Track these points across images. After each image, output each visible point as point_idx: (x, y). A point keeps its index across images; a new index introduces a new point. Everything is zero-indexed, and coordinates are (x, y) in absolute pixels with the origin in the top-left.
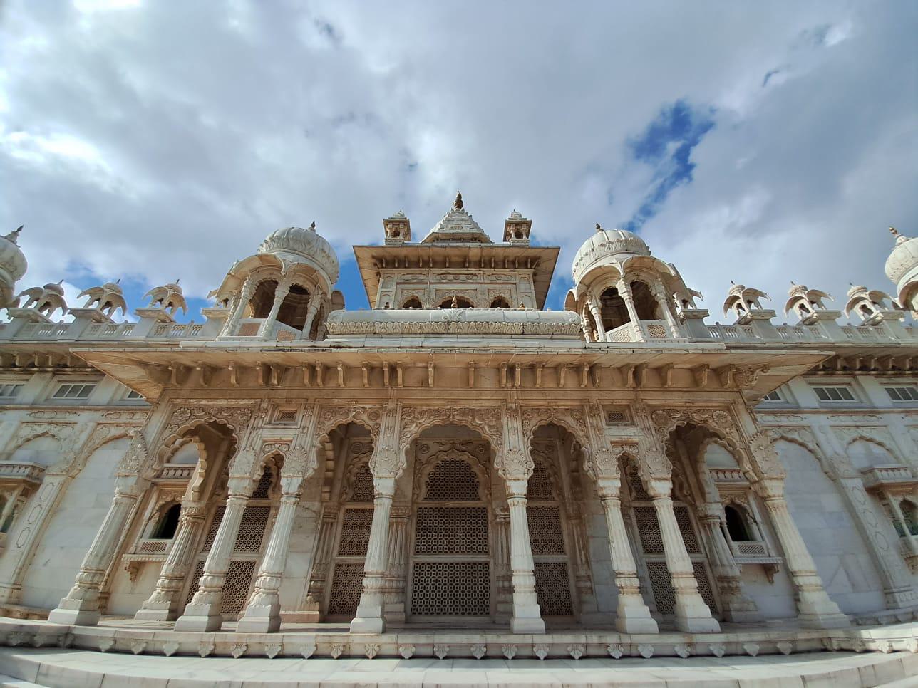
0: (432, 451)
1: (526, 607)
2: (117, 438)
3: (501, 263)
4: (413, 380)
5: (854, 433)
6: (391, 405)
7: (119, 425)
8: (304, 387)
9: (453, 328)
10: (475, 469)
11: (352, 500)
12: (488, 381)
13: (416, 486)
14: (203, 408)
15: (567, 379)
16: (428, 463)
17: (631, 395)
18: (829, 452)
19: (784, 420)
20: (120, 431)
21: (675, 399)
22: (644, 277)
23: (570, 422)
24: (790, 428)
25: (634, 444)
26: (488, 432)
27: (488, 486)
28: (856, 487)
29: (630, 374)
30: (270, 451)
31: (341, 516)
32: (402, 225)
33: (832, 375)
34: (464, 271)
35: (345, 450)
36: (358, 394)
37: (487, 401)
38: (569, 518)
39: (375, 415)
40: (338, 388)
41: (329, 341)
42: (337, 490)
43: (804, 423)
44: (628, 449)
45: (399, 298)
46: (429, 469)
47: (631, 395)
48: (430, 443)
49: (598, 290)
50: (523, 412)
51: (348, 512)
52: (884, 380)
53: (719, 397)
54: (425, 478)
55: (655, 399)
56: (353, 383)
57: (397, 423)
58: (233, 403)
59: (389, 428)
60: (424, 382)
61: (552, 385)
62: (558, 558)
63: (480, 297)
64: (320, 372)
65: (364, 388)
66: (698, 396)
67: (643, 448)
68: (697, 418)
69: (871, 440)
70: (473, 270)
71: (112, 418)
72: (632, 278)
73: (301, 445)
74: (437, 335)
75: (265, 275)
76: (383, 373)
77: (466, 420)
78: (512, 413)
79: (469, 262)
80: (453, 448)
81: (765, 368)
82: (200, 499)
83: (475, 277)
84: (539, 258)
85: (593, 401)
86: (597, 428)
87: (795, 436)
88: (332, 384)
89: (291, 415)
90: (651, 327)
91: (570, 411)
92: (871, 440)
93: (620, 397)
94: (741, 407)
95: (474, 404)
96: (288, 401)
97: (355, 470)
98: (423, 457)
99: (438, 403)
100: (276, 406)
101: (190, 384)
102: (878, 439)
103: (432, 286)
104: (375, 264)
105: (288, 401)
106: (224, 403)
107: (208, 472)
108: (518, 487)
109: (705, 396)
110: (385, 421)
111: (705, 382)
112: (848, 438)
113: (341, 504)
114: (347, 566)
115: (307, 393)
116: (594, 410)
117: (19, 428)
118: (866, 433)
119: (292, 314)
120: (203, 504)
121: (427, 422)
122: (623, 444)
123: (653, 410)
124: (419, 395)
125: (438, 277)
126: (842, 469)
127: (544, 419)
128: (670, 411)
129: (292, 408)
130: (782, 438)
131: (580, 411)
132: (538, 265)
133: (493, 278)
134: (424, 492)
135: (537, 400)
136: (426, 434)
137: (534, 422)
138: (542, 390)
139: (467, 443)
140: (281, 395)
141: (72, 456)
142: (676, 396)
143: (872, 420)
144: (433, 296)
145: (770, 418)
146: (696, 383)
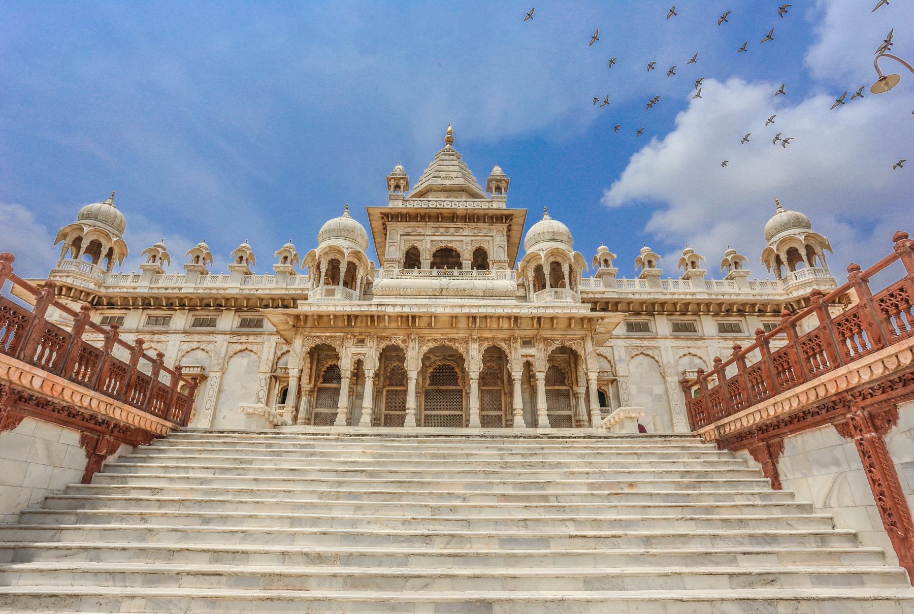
0: (433, 360)
2: (241, 351)
3: (482, 218)
4: (423, 324)
5: (686, 351)
6: (413, 337)
7: (241, 343)
8: (367, 327)
9: (444, 293)
10: (457, 370)
11: (389, 385)
12: (463, 324)
13: (424, 378)
14: (318, 337)
15: (505, 324)
16: (430, 366)
17: (536, 332)
18: (665, 361)
20: (243, 347)
21: (557, 334)
22: (559, 259)
23: (503, 345)
25: (533, 356)
26: (461, 350)
27: (464, 379)
28: (673, 382)
29: (535, 321)
30: (356, 358)
31: (385, 393)
32: (402, 181)
33: (684, 314)
34: (452, 225)
35: (383, 359)
36: (396, 331)
37: (462, 334)
38: (505, 394)
39: (404, 341)
40: (385, 328)
41: (376, 300)
42: (382, 379)
43: (657, 345)
44: (530, 359)
45: (402, 248)
46: (431, 370)
47: (536, 332)
48: (431, 356)
49: (533, 265)
50: (481, 340)
51: (388, 391)
52: (719, 318)
53: (579, 333)
54: (428, 375)
55: (547, 334)
56: (393, 325)
57: (417, 346)
58: (333, 334)
59: (413, 348)
60: (430, 325)
61: (496, 326)
62: (499, 413)
63: (465, 248)
64: (374, 319)
65: (398, 328)
66: (570, 332)
67: (537, 357)
68: (567, 344)
69: (695, 355)
70: (459, 225)
71: (236, 339)
72: (552, 259)
73: (371, 354)
74: (435, 296)
75: (332, 256)
76: (409, 320)
77: (451, 344)
78: (474, 341)
79: (457, 217)
80: (444, 358)
81: (602, 319)
82: (310, 383)
83: (461, 230)
84: (512, 215)
85: (516, 335)
86: (516, 349)
87: (650, 352)
88: (382, 325)
89: (362, 341)
90: (556, 292)
91: (504, 340)
92: (695, 355)
93: (530, 333)
94: (589, 339)
95: (455, 336)
96: (361, 334)
97: (389, 370)
98: (427, 363)
99: (438, 335)
100: (354, 336)
101: (309, 324)
102: (699, 355)
103: (428, 238)
104: (383, 218)
105: (361, 334)
106: (328, 334)
107: (311, 369)
109: (573, 332)
111: (573, 326)
112: (681, 354)
113: (384, 387)
114: (391, 415)
115: (369, 330)
116: (515, 339)
117: (180, 345)
118: (693, 351)
119: (350, 282)
120: (312, 385)
121: (432, 345)
122: (526, 356)
123: (546, 339)
124: (426, 331)
125: (433, 230)
126: (669, 371)
127: (490, 344)
128: (553, 340)
129: (363, 337)
130: (642, 353)
132: (511, 220)
133: (476, 231)
134: (428, 381)
135: (487, 334)
136: (431, 351)
137: (486, 345)
138: (490, 329)
139: (452, 356)
140: (357, 330)
141: (221, 361)
142: (558, 332)
143: (699, 343)
144: (429, 247)
145: (638, 341)
146: (570, 325)
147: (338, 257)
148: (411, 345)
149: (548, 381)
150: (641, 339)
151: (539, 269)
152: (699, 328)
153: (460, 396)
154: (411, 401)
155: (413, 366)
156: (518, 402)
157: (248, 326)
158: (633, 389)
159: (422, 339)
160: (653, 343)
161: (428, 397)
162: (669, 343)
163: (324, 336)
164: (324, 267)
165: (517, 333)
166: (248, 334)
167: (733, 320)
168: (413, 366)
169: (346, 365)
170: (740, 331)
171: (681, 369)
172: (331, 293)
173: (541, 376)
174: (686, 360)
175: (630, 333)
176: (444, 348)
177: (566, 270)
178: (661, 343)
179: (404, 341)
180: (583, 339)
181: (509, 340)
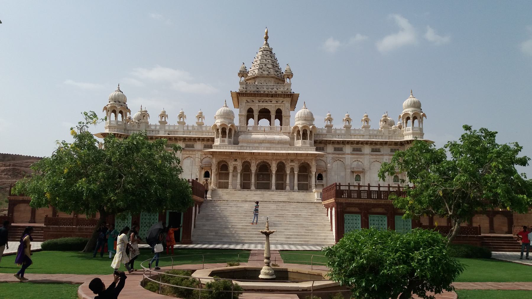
1: (274, 187)
19: (340, 156)
21: (303, 158)
22: (306, 128)
23: (284, 161)
24: (341, 158)
26: (270, 163)
28: (349, 171)
39: (250, 160)
49: (297, 130)
50: (276, 160)
53: (311, 158)
55: (299, 158)
72: (304, 128)
73: (239, 165)
78: (274, 160)
93: (293, 158)
108: (274, 172)
110: (253, 161)
116: (288, 160)
118: (359, 159)
121: (260, 161)
128: (301, 160)
131: (286, 160)
135: (278, 158)
137: (278, 162)
143: (362, 156)
147: (225, 127)
148: (253, 161)
149: (300, 171)
150: (339, 154)
151: (299, 131)
152: (363, 150)
153: (269, 176)
154: (253, 180)
155: (253, 169)
156: (288, 181)
157: (189, 147)
158: (333, 174)
159: (256, 159)
160: (343, 156)
161: (257, 175)
162: (350, 156)
163: (223, 158)
164: (220, 131)
165: (289, 157)
166: (189, 151)
167: (378, 147)
168: (253, 169)
169: (231, 169)
170: (380, 152)
171: (353, 166)
172: (223, 141)
173: (296, 173)
174: (356, 163)
175: (335, 152)
176: (264, 162)
177: (308, 133)
178: (347, 156)
179: (250, 160)
180: (312, 160)
181: (286, 160)
